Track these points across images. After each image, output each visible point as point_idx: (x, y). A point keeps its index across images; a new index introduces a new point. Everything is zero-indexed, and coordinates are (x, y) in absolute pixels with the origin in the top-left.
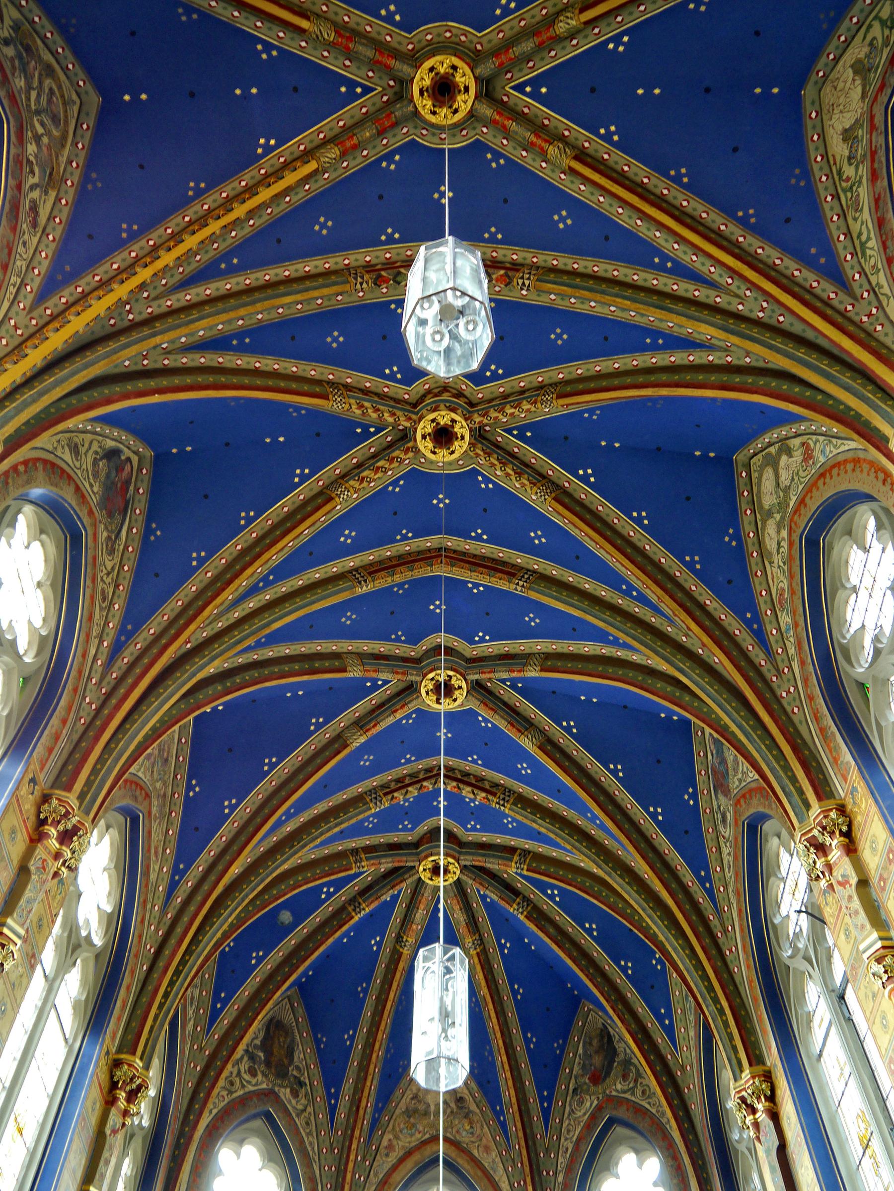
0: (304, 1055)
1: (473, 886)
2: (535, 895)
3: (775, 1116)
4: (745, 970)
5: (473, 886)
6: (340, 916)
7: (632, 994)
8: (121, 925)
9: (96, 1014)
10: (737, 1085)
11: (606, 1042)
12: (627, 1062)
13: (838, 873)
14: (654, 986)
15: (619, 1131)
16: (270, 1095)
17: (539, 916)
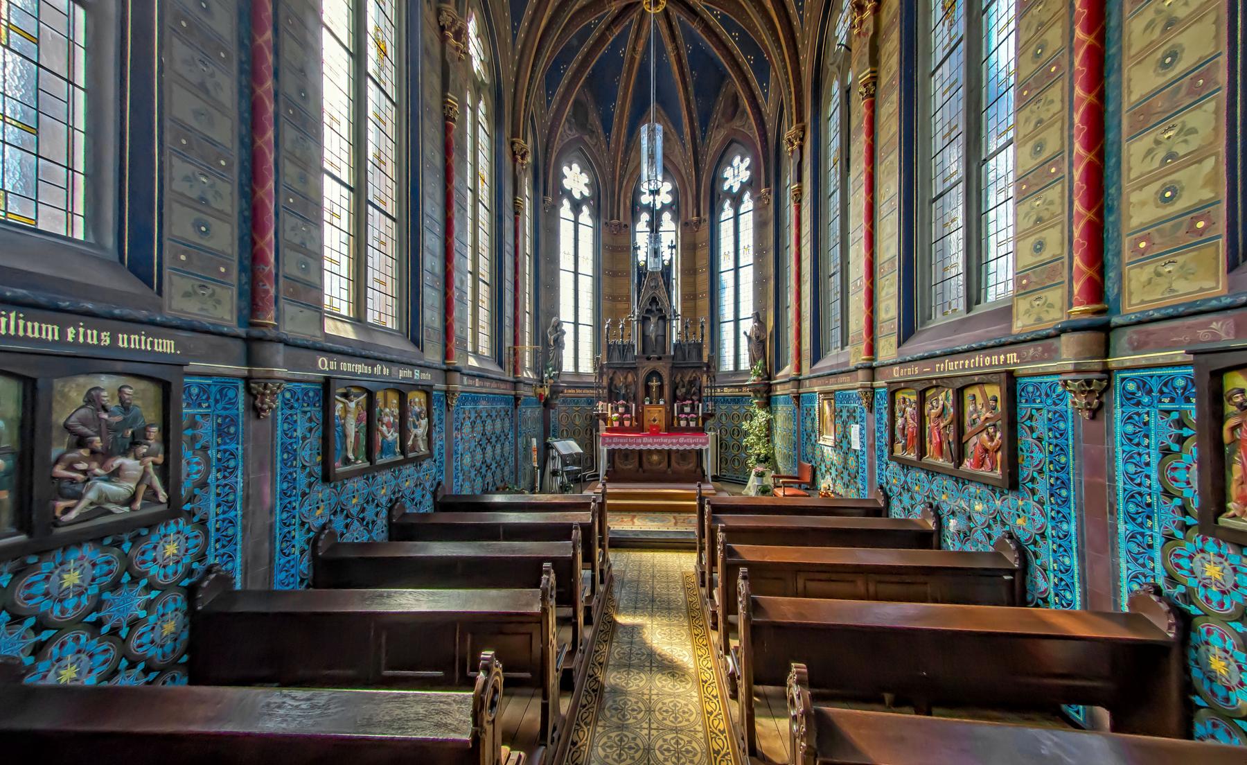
0: (594, 119)
1: (674, 13)
2: (707, 15)
3: (801, 147)
4: (807, 70)
5: (674, 13)
6: (601, 40)
7: (751, 75)
8: (492, 64)
9: (497, 118)
10: (789, 132)
11: (736, 98)
12: (744, 111)
13: (864, 27)
14: (762, 68)
15: (735, 145)
16: (580, 140)
17: (708, 29)
